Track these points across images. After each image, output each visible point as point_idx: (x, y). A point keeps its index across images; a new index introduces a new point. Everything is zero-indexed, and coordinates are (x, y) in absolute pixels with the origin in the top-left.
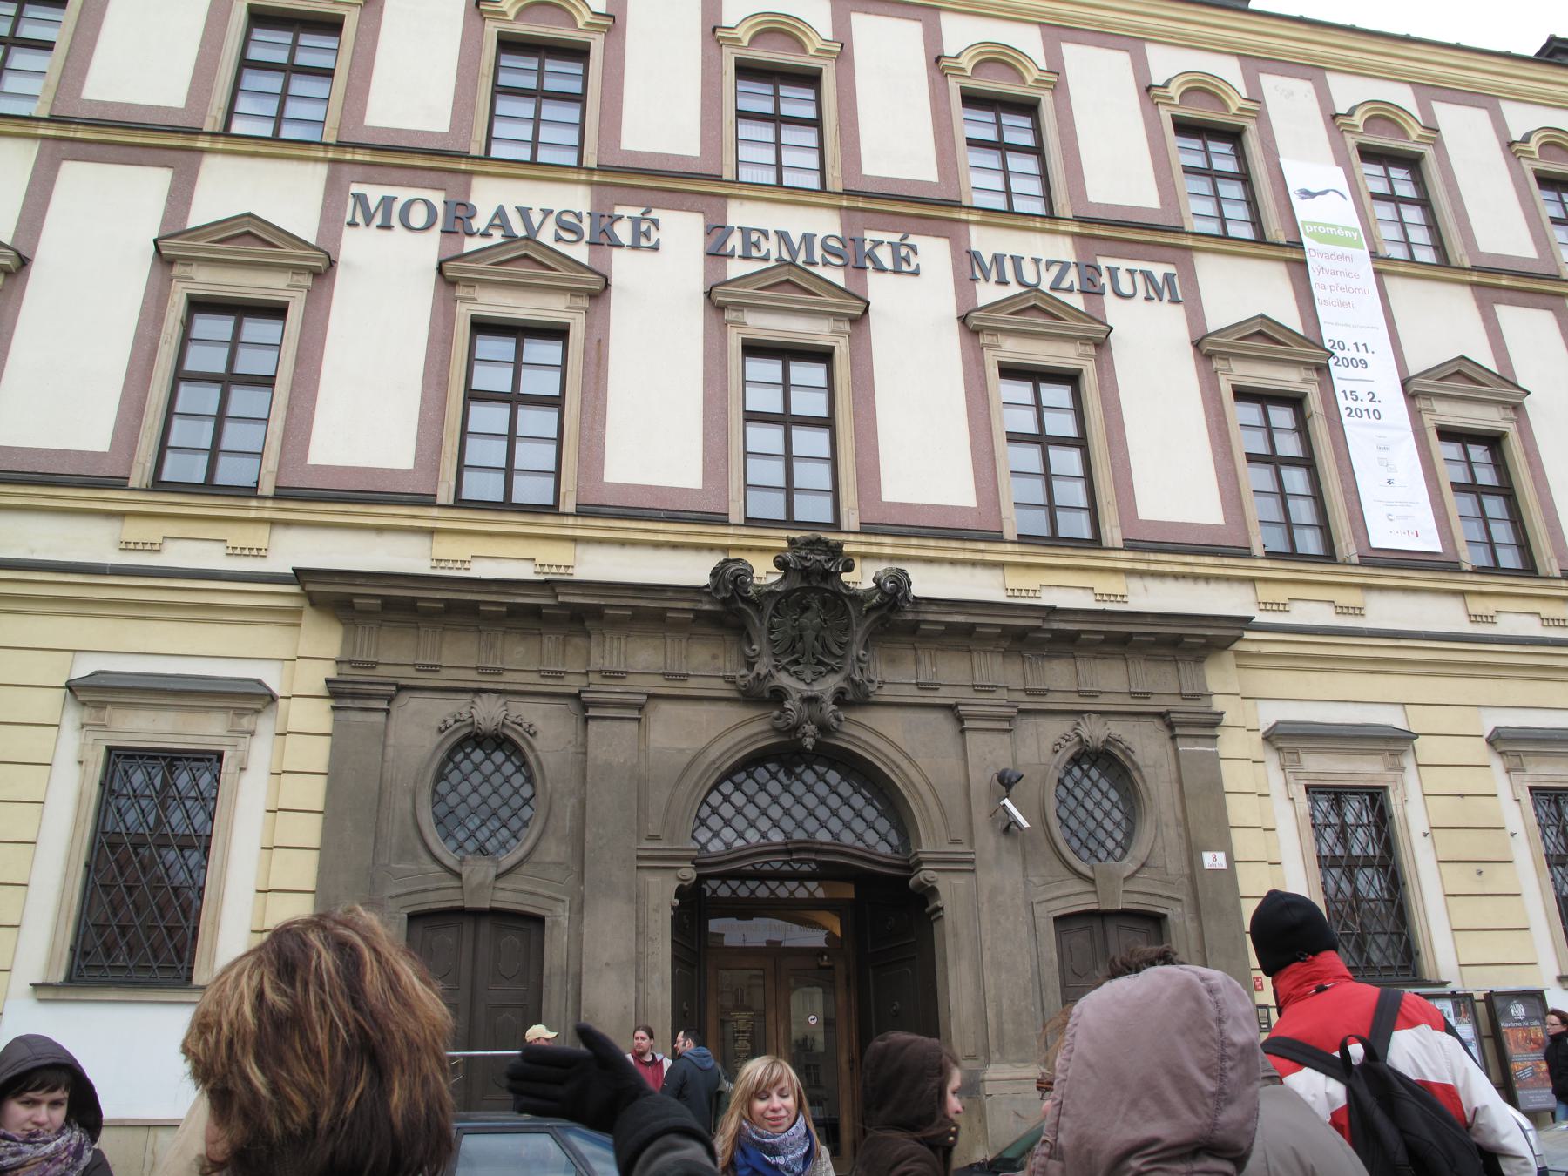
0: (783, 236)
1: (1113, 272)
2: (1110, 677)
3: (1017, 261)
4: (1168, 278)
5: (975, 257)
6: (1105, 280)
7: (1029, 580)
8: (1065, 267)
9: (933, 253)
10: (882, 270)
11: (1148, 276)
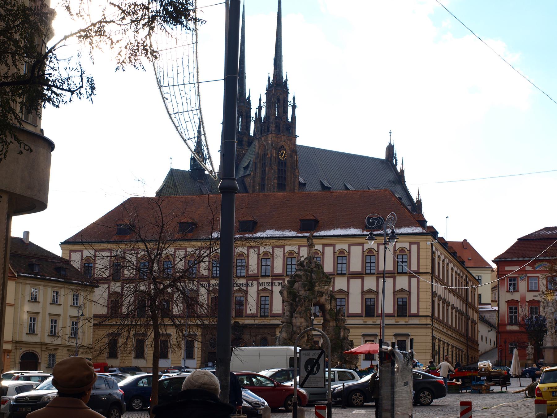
0: (240, 283)
1: (275, 283)
2: (266, 331)
3: (264, 283)
4: (281, 282)
5: (260, 283)
6: (274, 284)
7: (260, 321)
8: (270, 283)
9: (255, 283)
10: (249, 286)
11: (279, 282)
